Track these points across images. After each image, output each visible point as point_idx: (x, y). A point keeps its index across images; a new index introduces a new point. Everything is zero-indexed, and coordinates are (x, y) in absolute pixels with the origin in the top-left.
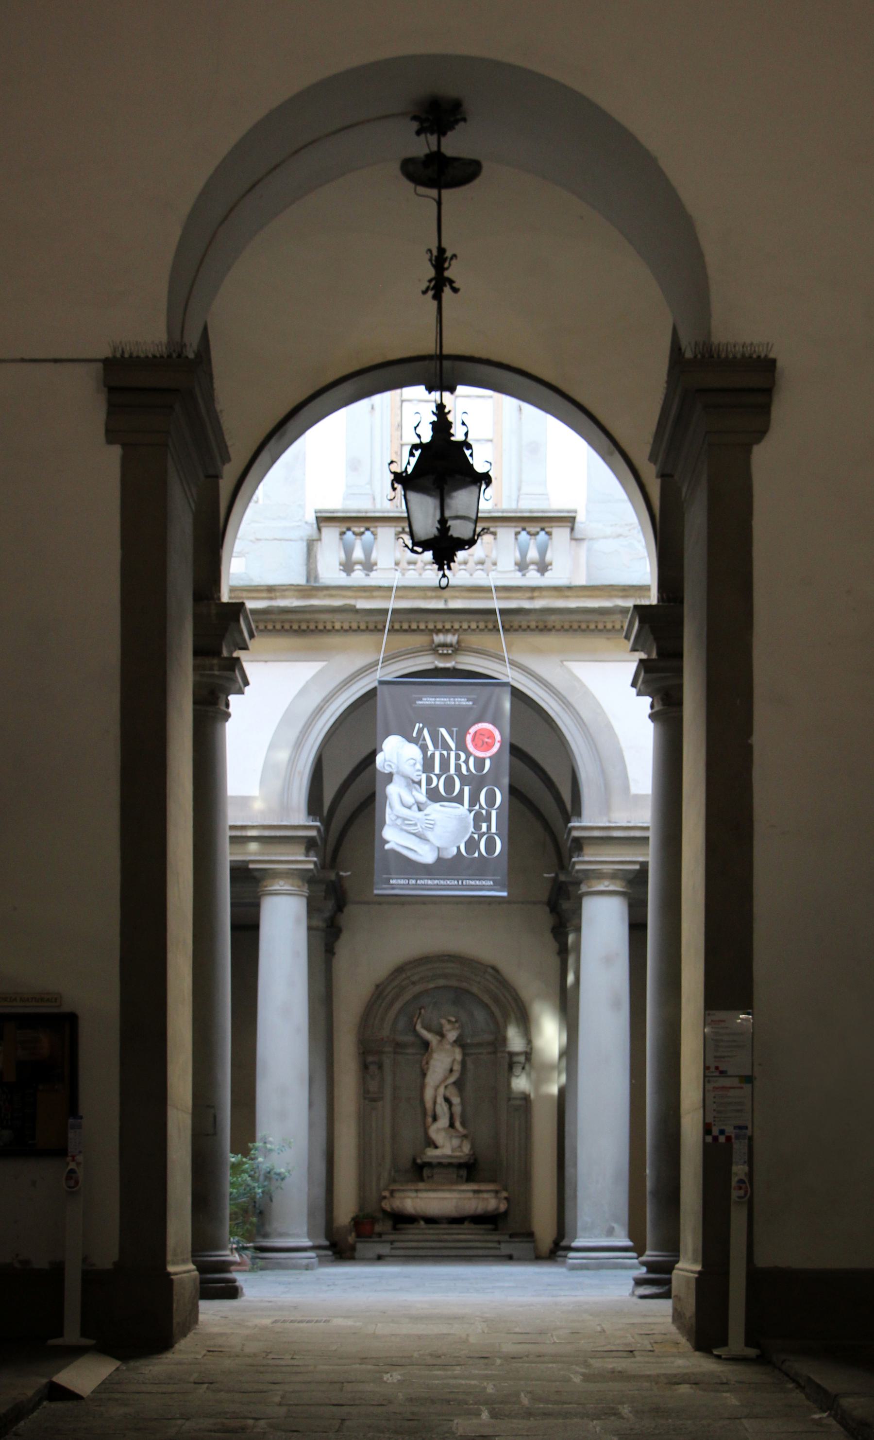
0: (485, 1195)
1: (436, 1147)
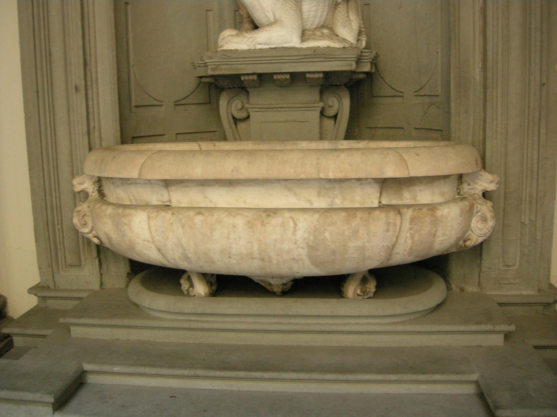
0: (425, 196)
1: (256, 27)
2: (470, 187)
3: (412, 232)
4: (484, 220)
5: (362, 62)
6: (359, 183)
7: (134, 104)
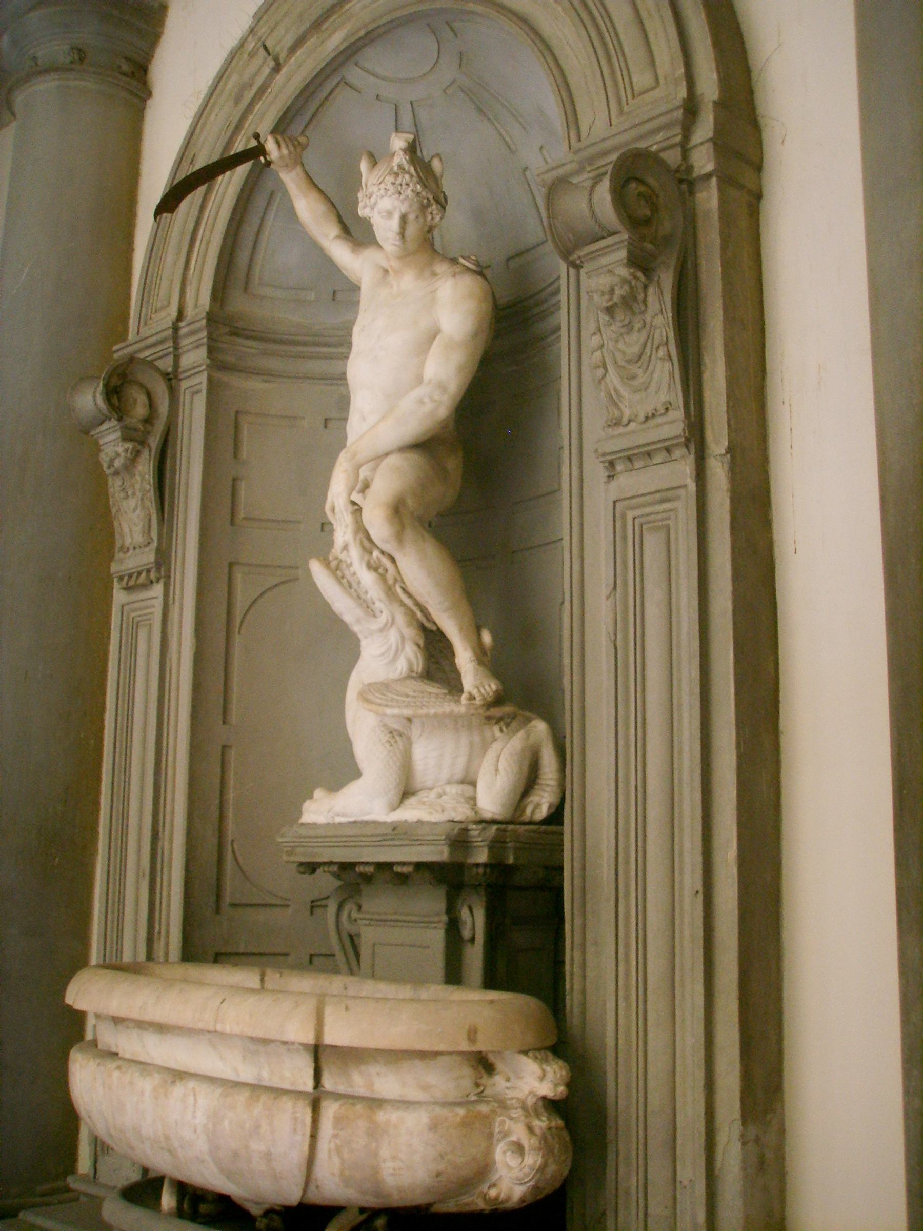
2: (508, 1085)
3: (338, 1142)
4: (519, 1148)
5: (475, 847)
6: (286, 1047)
7: (227, 899)
